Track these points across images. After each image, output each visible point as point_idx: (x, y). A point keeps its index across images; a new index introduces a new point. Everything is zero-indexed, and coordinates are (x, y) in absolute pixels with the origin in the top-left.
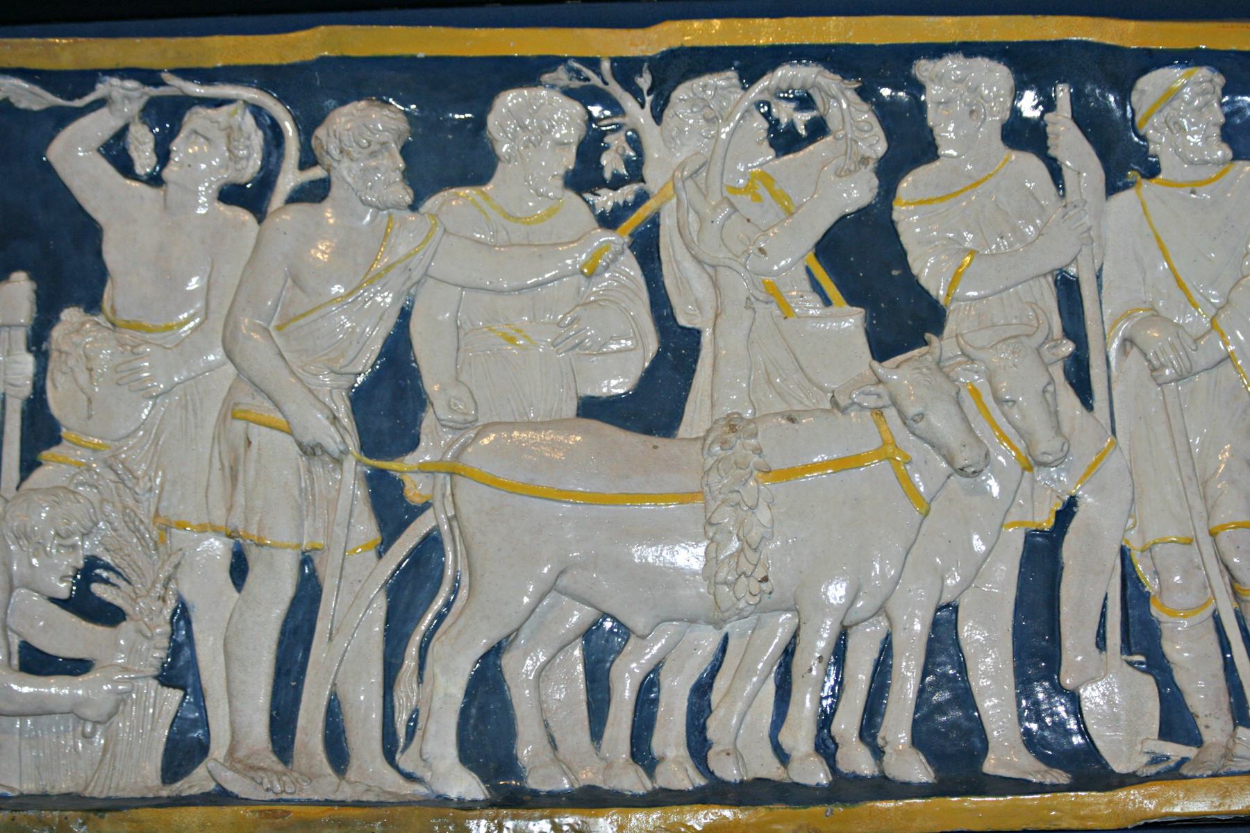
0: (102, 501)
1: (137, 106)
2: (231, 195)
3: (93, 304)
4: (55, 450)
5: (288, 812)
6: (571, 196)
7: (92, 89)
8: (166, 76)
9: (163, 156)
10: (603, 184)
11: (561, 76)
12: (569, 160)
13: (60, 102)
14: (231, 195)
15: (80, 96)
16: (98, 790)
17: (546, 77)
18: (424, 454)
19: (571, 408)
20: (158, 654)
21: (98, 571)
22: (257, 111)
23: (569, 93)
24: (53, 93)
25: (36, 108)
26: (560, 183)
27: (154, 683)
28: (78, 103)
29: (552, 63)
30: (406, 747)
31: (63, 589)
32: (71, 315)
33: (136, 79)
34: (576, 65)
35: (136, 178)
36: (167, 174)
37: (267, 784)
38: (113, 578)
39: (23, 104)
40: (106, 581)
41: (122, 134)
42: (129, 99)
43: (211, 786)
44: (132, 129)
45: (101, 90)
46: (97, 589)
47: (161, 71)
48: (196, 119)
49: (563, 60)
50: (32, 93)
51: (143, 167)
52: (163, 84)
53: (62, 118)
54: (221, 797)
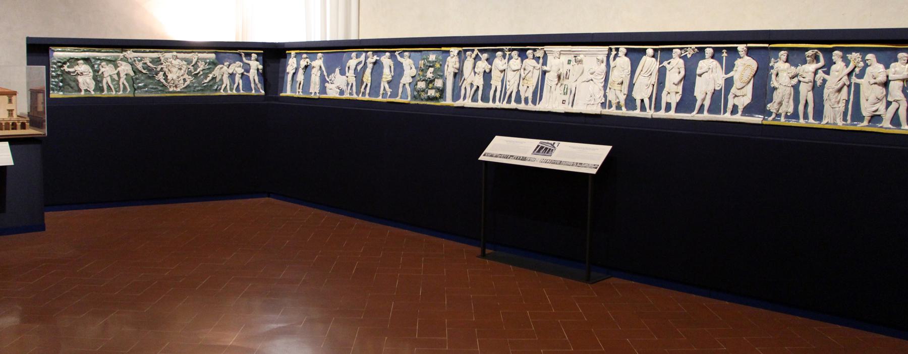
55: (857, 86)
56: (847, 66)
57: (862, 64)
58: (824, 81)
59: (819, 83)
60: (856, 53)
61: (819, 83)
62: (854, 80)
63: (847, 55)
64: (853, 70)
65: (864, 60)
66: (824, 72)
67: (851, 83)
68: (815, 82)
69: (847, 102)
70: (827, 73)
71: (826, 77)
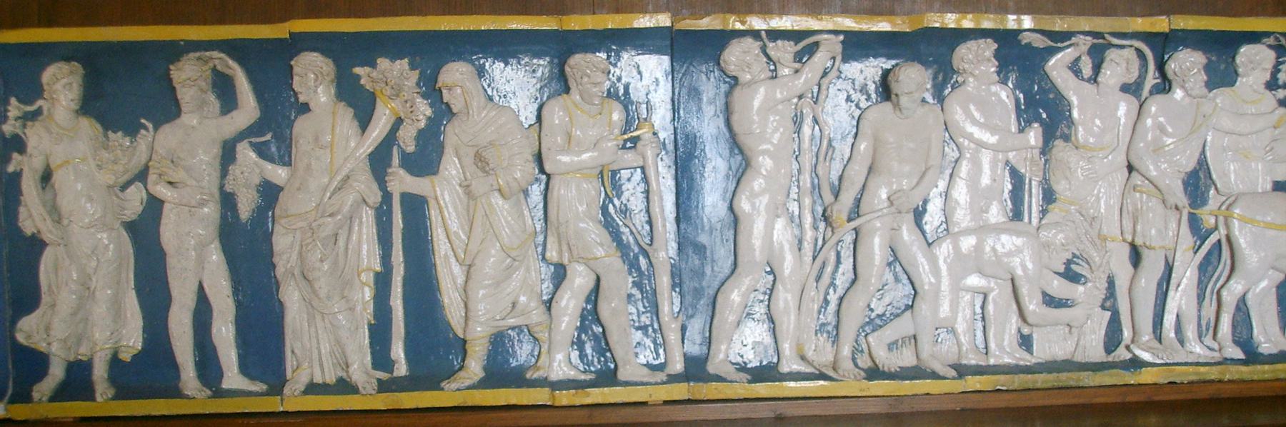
0: (1076, 228)
1: (1085, 48)
2: (1125, 88)
3: (1066, 138)
4: (565, 95)
5: (1174, 369)
6: (1268, 92)
7: (1070, 39)
8: (1106, 35)
9: (1097, 68)
10: (1279, 87)
11: (1271, 41)
12: (1268, 76)
13: (1055, 45)
14: (1125, 88)
15: (1063, 42)
16: (1079, 358)
17: (1265, 40)
18: (1207, 208)
19: (1269, 186)
20: (1101, 294)
21: (1075, 259)
22: (1138, 51)
23: (1270, 47)
24: (1052, 41)
25: (1042, 47)
26: (1264, 86)
27: (1100, 309)
28: (1059, 45)
29: (1267, 34)
30: (1206, 335)
31: (1062, 269)
32: (1059, 143)
33: (1090, 36)
34: (1278, 36)
35: (1083, 79)
36: (1099, 79)
37: (1160, 355)
38: (1080, 262)
39: (1035, 45)
40: (1078, 264)
41: (1078, 59)
42: (1084, 44)
43: (1129, 356)
44: (1083, 58)
45: (1074, 40)
46: (1073, 267)
47: (1103, 33)
48: (1112, 54)
49: (1274, 33)
50: (1043, 41)
51: (1086, 74)
52: (1104, 38)
53: (1052, 51)
54: (1136, 364)
55: (416, 207)
56: (364, 120)
57: (424, 109)
58: (270, 193)
59: (246, 206)
60: (393, 59)
61: (246, 206)
62: (401, 182)
63: (358, 70)
64: (390, 139)
65: (431, 90)
66: (262, 151)
67: (387, 197)
68: (228, 201)
69: (382, 282)
70: (283, 153)
71: (279, 174)
